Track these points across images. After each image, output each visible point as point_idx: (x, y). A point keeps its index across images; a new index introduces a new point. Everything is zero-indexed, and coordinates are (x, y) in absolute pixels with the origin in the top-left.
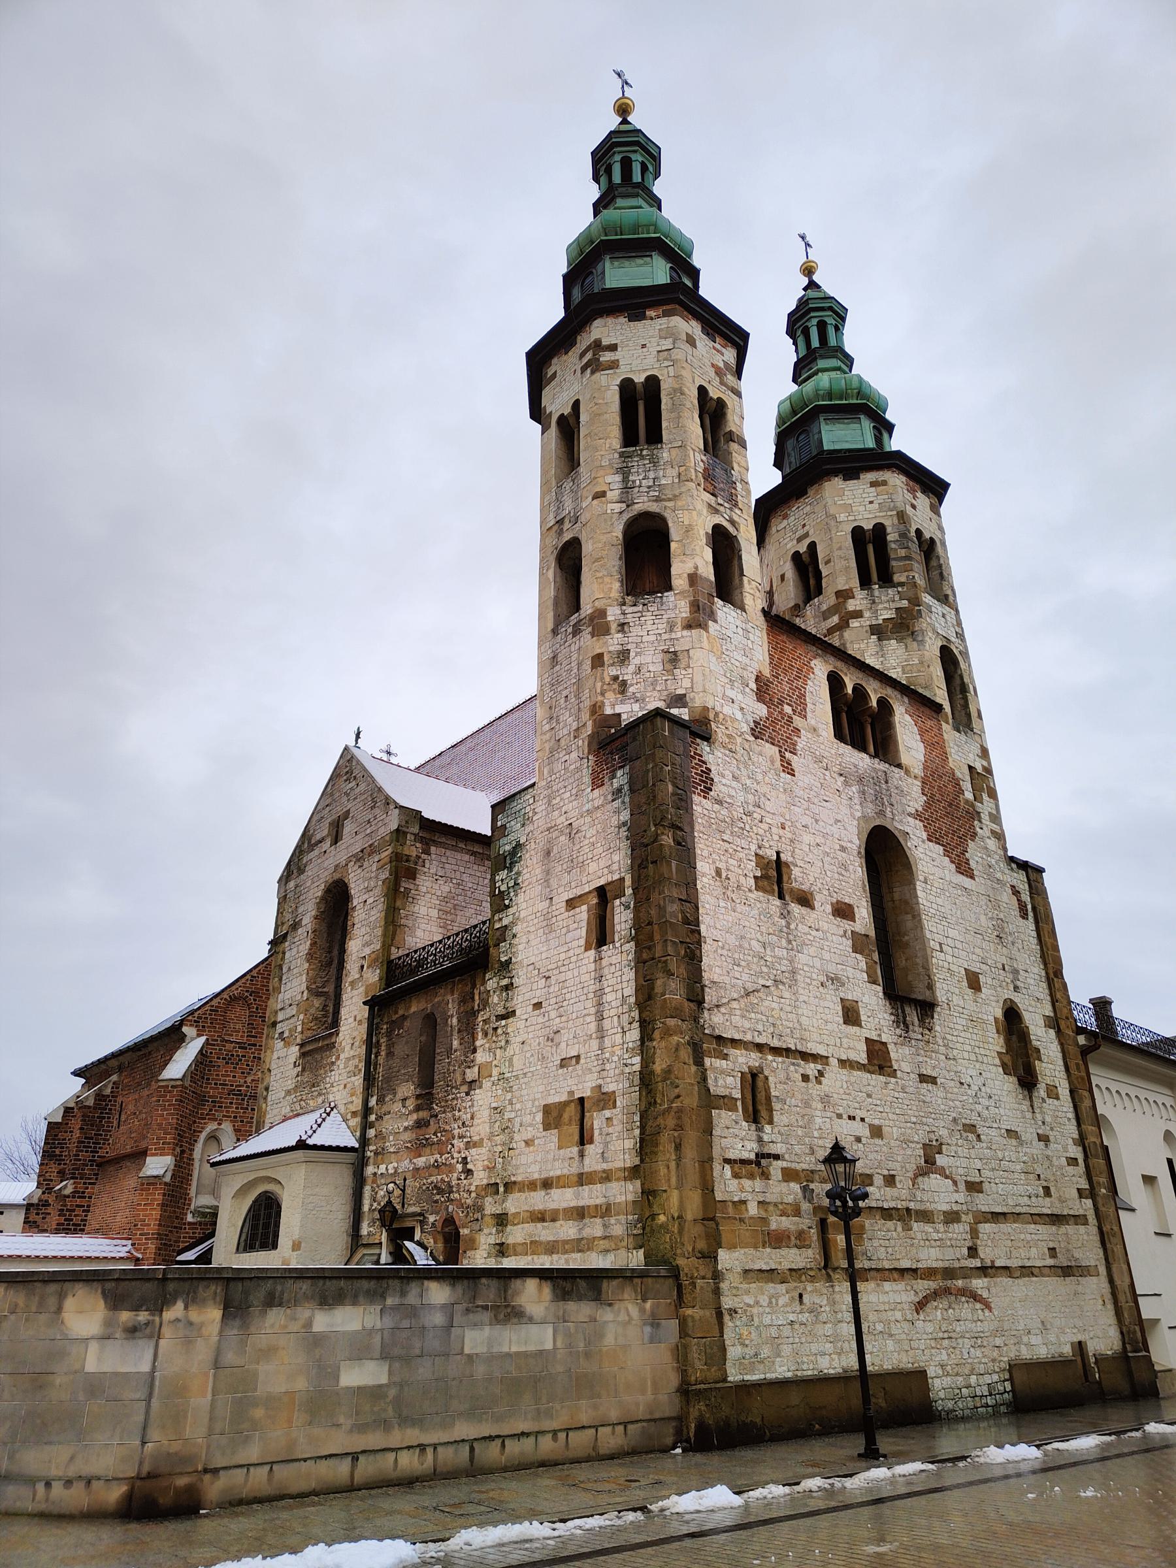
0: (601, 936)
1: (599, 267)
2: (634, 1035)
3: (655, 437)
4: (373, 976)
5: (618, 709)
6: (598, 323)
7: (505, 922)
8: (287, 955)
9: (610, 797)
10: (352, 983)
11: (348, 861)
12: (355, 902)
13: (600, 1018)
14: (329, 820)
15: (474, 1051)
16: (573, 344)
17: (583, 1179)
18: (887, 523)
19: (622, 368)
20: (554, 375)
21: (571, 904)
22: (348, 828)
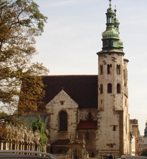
0: (114, 129)
1: (112, 41)
2: (119, 139)
3: (119, 74)
4: (75, 125)
5: (117, 107)
6: (115, 54)
7: (100, 125)
8: (51, 118)
9: (116, 117)
10: (70, 125)
11: (66, 108)
12: (69, 115)
13: (114, 137)
14: (59, 100)
15: (96, 137)
16: (110, 55)
17: (111, 150)
18: (125, 70)
19: (117, 63)
20: (107, 57)
21: (110, 126)
22: (65, 103)
